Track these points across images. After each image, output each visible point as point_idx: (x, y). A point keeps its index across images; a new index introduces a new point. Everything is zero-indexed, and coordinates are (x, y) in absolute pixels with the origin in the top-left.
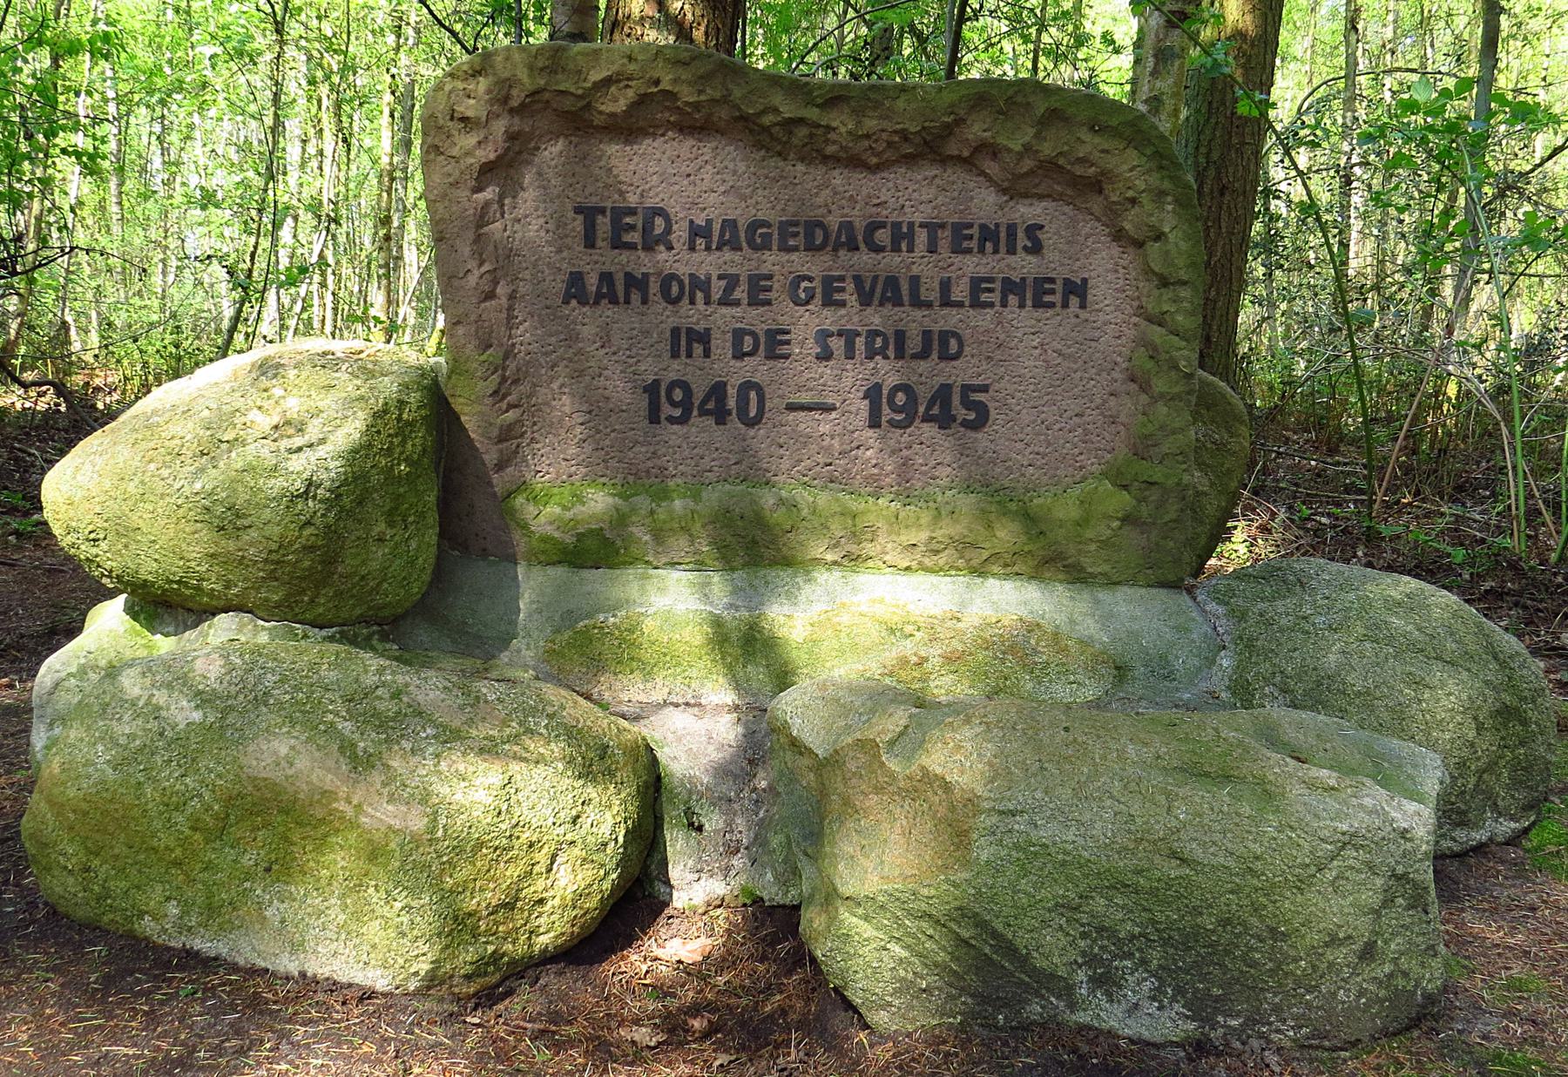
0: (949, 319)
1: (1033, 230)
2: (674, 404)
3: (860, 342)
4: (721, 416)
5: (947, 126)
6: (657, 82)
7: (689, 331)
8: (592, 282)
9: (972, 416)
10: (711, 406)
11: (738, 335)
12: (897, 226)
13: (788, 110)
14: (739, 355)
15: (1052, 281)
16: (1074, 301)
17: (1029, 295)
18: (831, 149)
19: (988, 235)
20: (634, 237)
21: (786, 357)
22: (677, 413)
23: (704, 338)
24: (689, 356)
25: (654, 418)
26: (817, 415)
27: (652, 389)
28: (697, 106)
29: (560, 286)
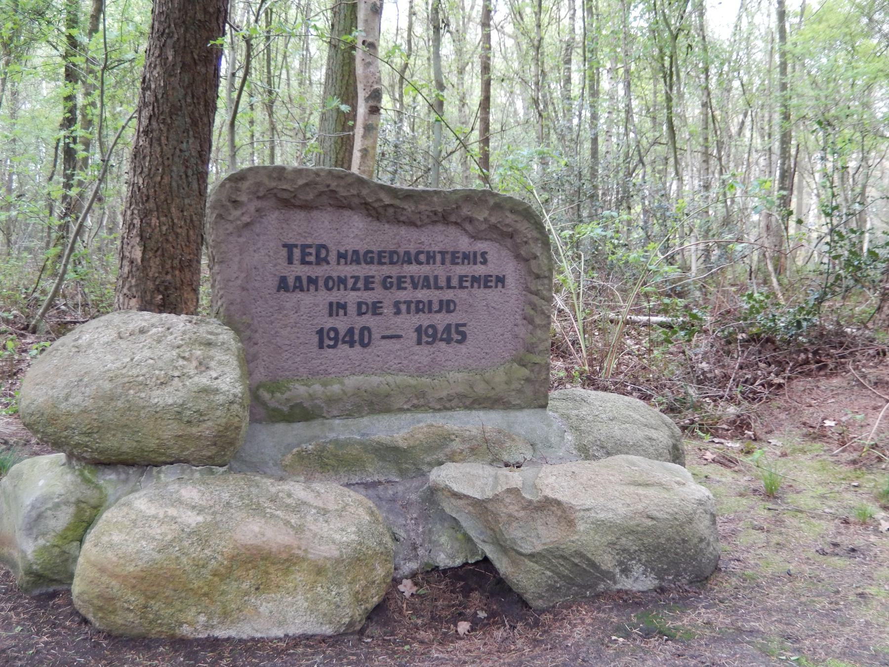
0: (448, 295)
1: (484, 254)
2: (330, 339)
3: (413, 306)
4: (352, 344)
5: (453, 209)
6: (328, 186)
7: (338, 303)
8: (291, 281)
9: (460, 338)
10: (347, 339)
11: (359, 304)
12: (428, 252)
13: (387, 201)
14: (360, 314)
15: (491, 276)
16: (500, 285)
17: (482, 283)
18: (402, 218)
19: (466, 256)
20: (312, 259)
21: (381, 314)
22: (332, 343)
23: (343, 306)
24: (337, 315)
25: (321, 346)
26: (394, 341)
27: (320, 332)
28: (345, 198)
29: (276, 283)
